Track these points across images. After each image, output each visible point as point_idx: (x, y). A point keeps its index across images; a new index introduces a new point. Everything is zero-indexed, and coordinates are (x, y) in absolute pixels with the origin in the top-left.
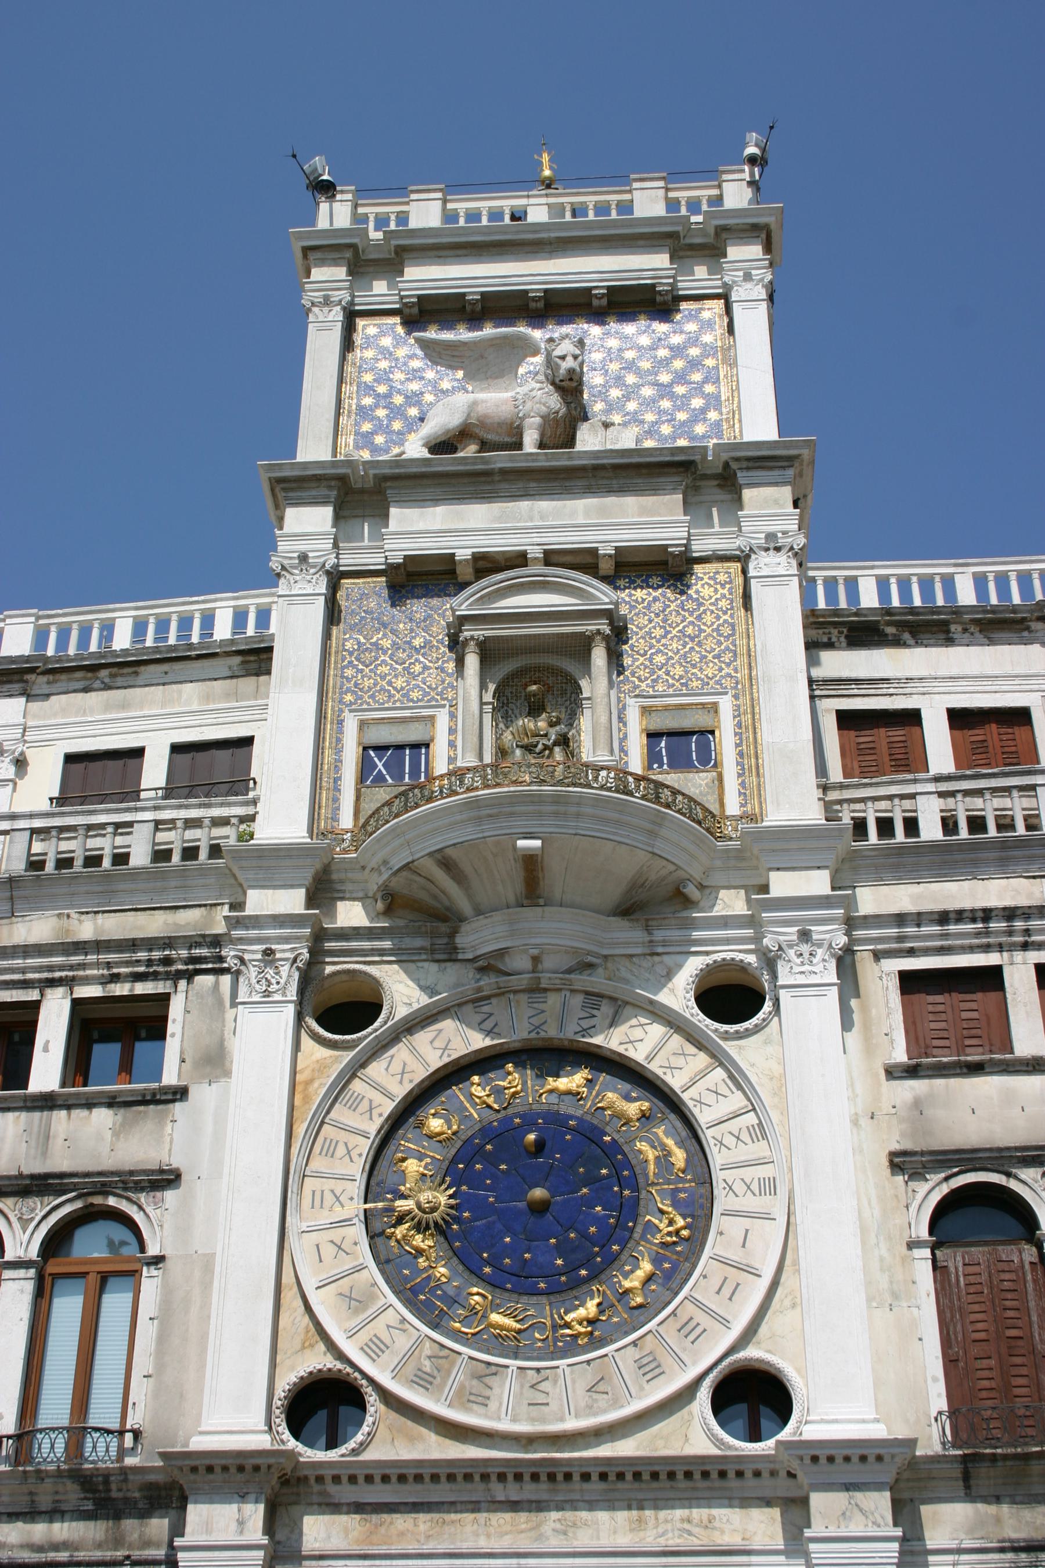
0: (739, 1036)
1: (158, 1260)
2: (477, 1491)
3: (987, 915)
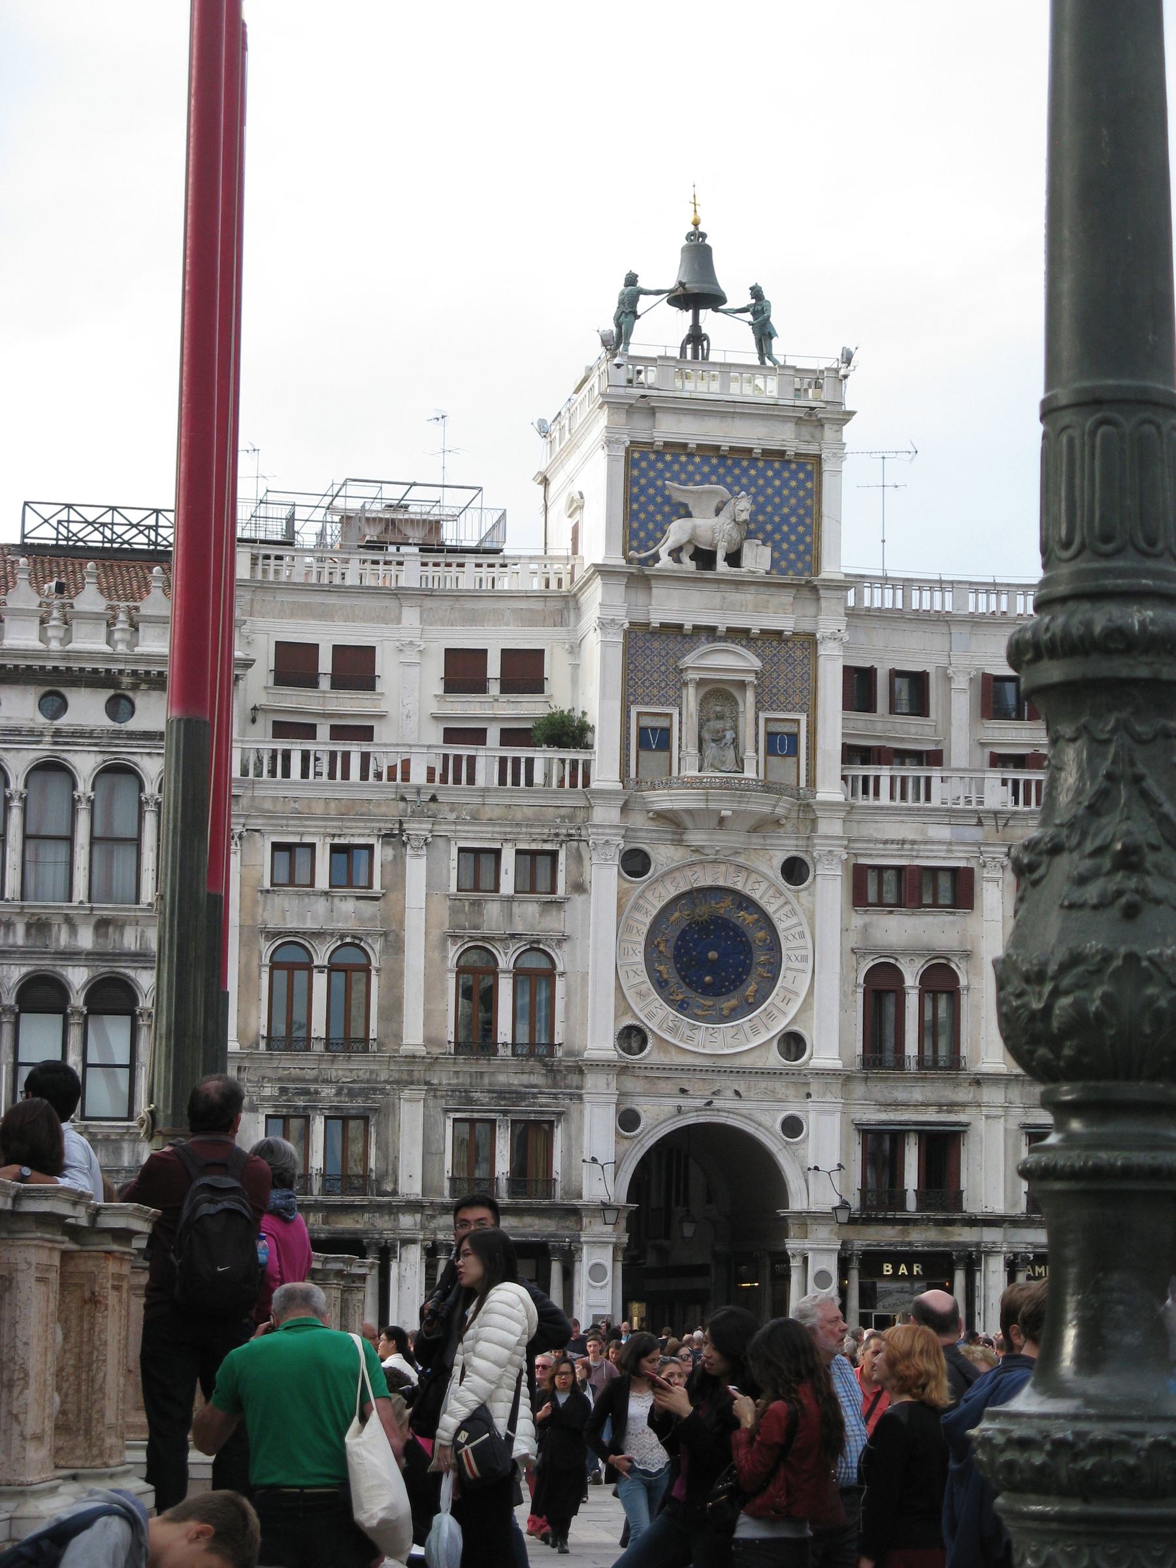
0: (798, 891)
1: (562, 974)
3: (903, 842)
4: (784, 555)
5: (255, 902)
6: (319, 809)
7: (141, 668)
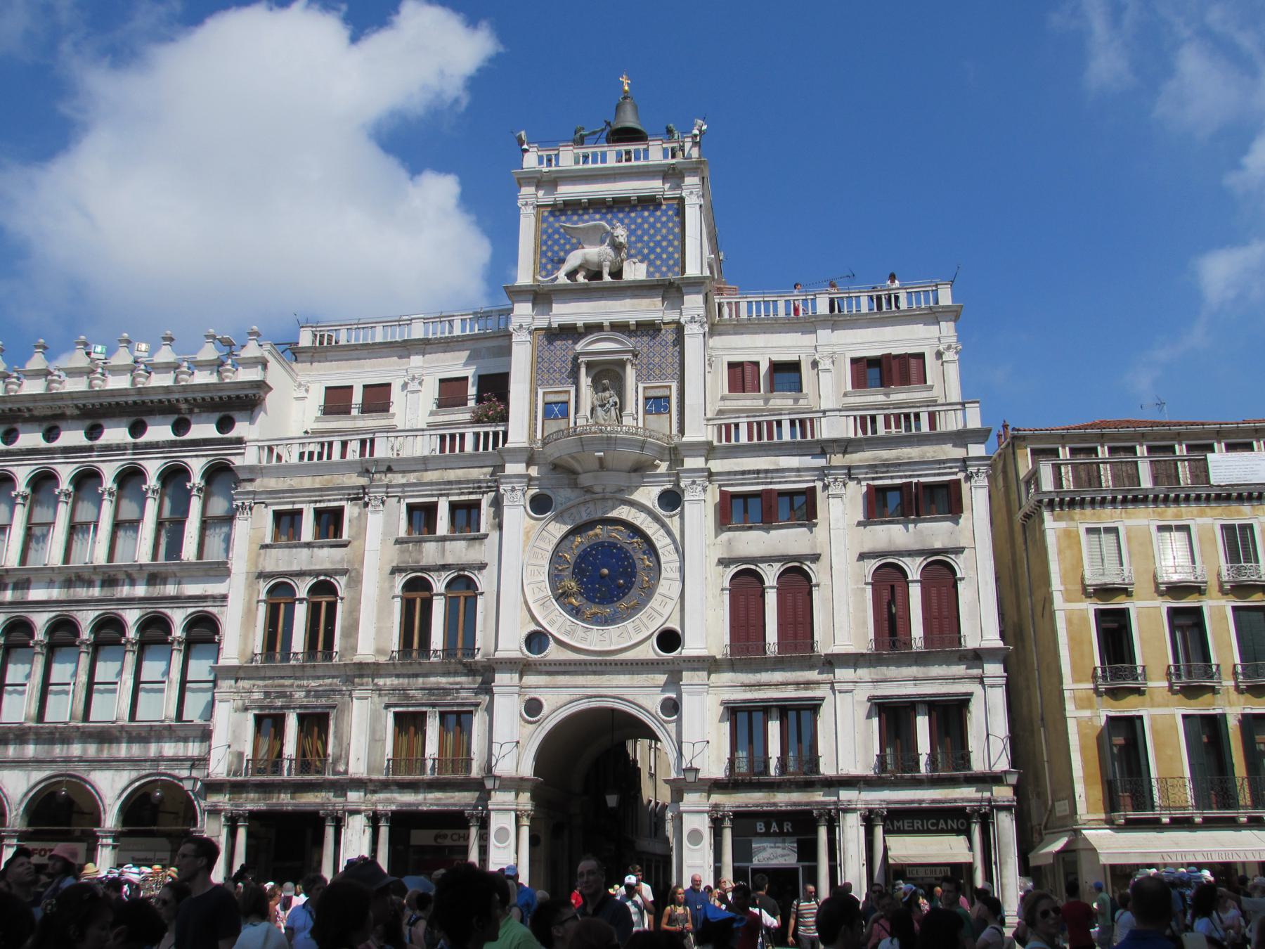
0: (671, 517)
1: (482, 594)
2: (583, 668)
3: (758, 472)
4: (658, 269)
5: (259, 555)
7: (190, 396)
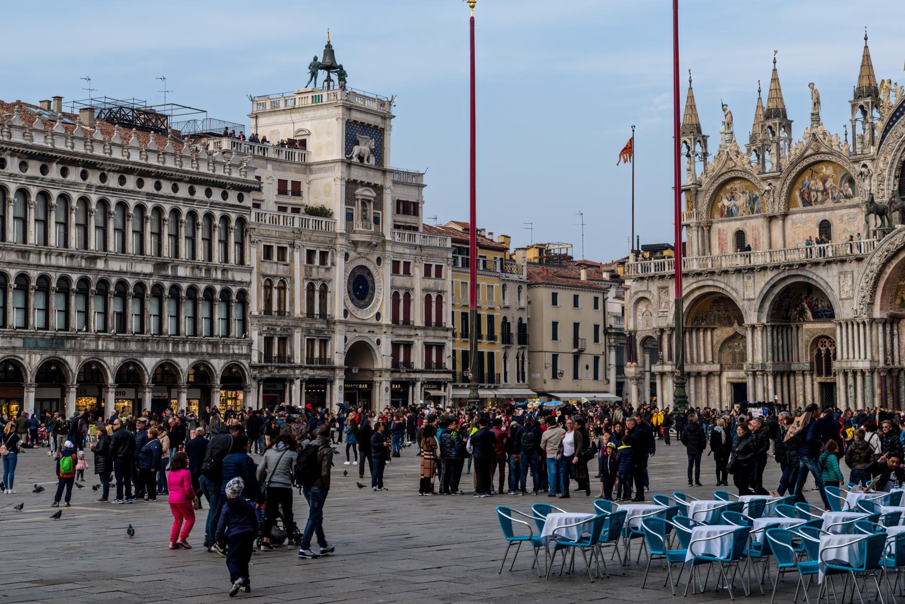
6: (274, 234)
